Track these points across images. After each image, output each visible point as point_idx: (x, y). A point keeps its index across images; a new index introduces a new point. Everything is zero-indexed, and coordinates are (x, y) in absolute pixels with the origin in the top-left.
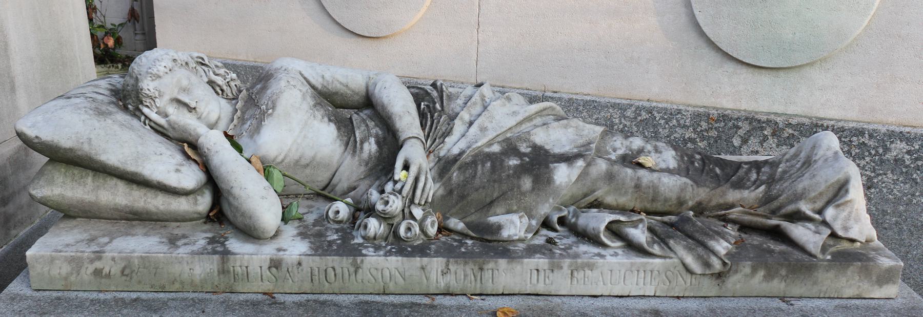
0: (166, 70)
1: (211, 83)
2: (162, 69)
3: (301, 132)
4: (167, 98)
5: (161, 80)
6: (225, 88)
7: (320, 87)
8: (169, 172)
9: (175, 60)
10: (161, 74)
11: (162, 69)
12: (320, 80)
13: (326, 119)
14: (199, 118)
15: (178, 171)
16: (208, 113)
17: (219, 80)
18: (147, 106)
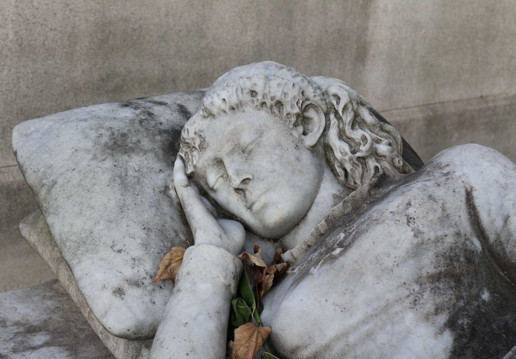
0: (223, 106)
1: (323, 151)
2: (218, 102)
3: (364, 322)
4: (209, 154)
5: (214, 121)
6: (348, 167)
7: (492, 238)
8: (104, 287)
9: (253, 93)
10: (215, 111)
11: (218, 102)
12: (499, 223)
13: (443, 318)
14: (250, 208)
15: (119, 292)
16: (265, 206)
17: (340, 149)
18: (182, 158)
